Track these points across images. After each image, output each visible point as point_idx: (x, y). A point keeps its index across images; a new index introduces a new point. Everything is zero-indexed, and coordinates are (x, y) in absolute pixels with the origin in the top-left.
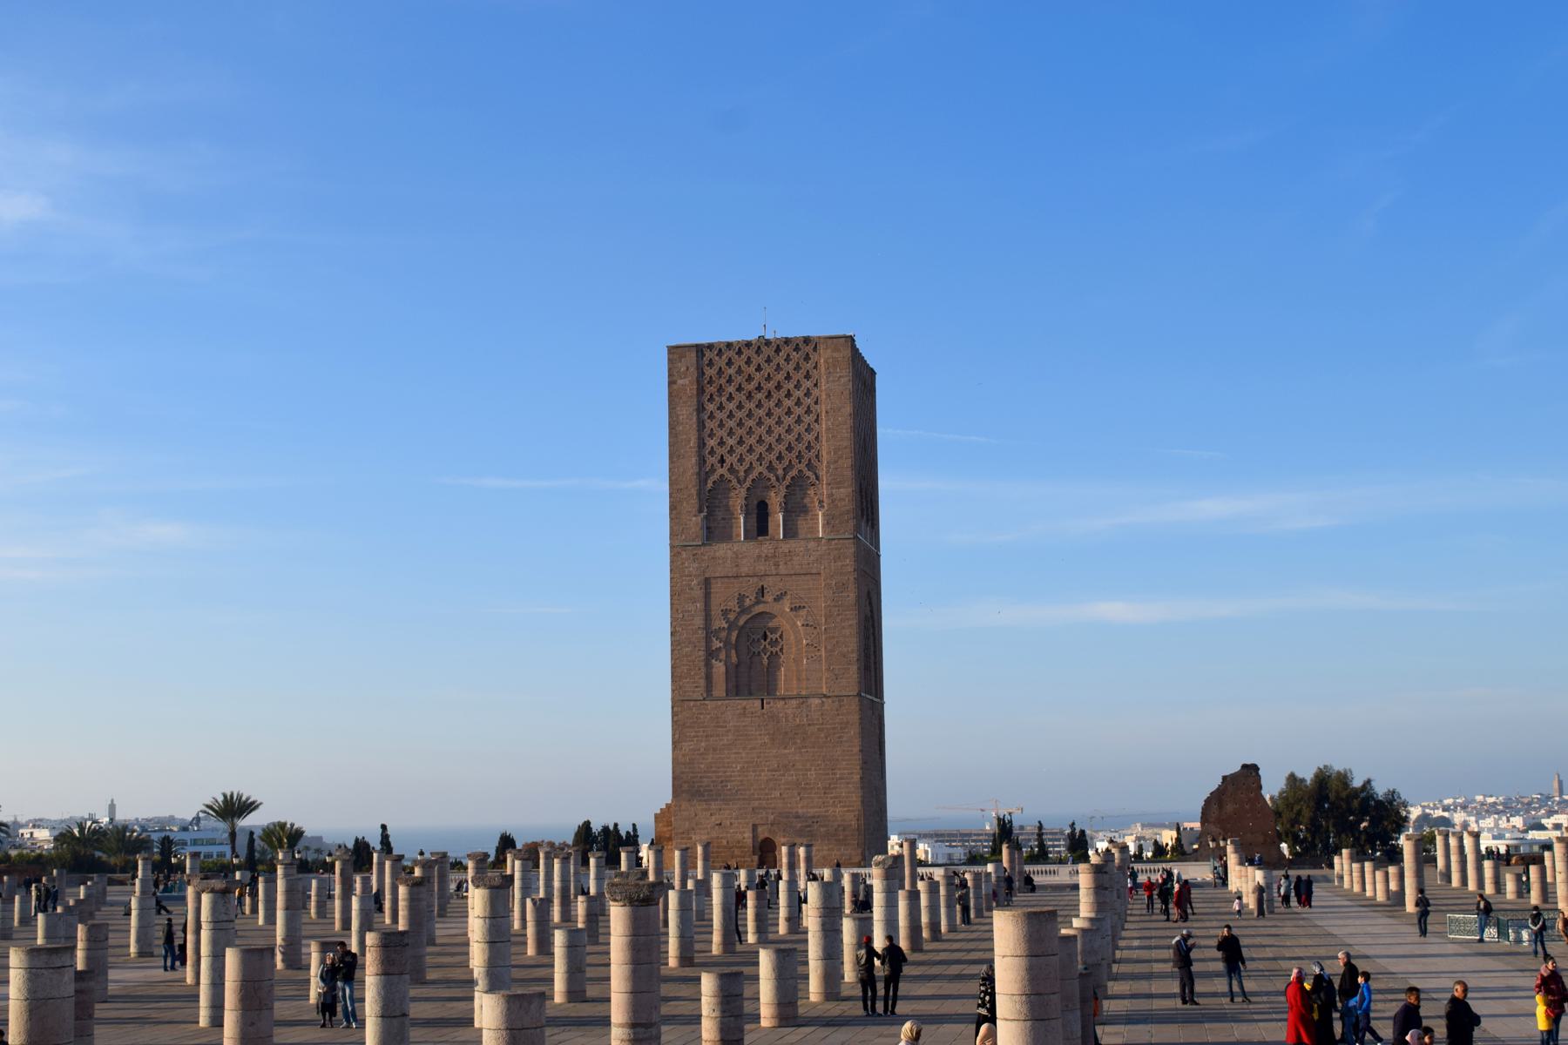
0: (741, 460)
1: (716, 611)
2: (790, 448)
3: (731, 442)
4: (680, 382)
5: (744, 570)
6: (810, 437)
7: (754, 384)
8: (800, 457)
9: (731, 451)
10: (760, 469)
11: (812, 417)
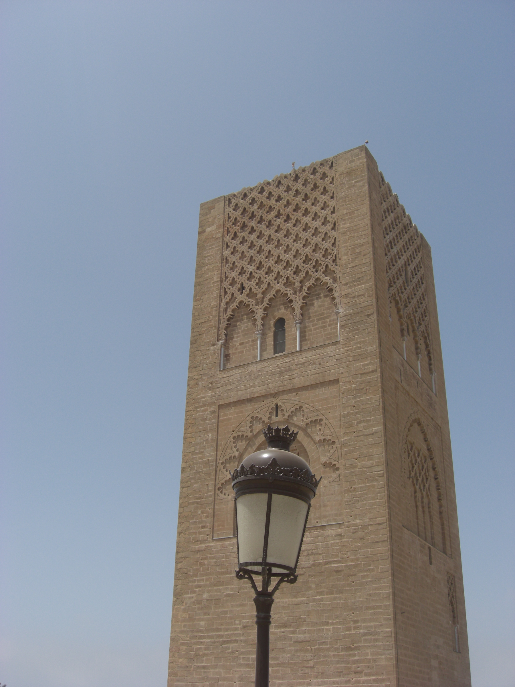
0: (259, 283)
2: (307, 260)
3: (251, 268)
4: (208, 230)
5: (258, 390)
6: (327, 245)
7: (274, 213)
10: (277, 287)
11: (329, 227)
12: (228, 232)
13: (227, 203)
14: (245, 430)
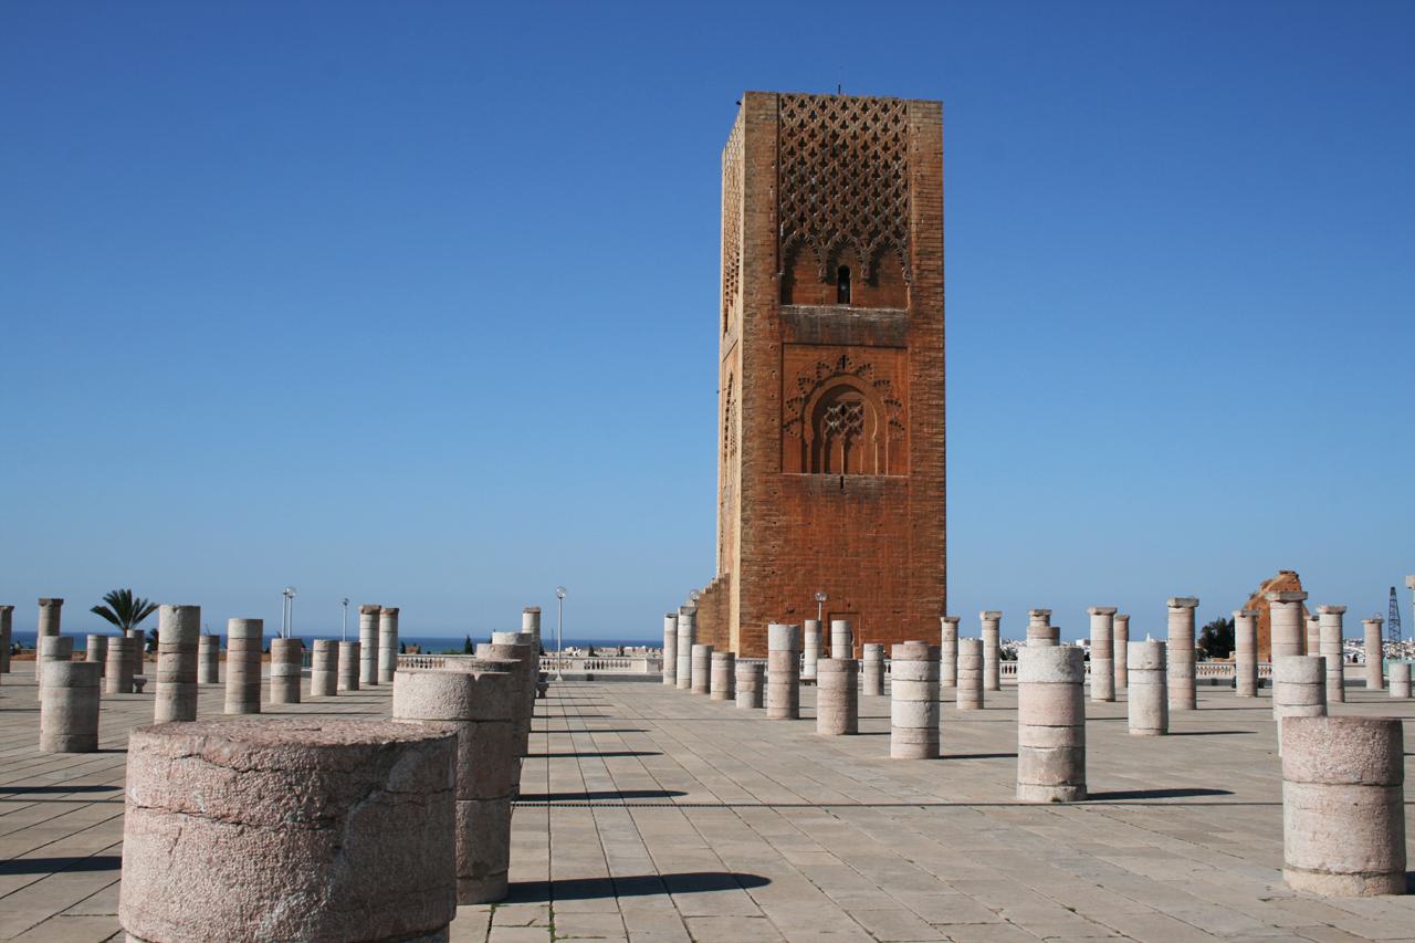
0: (823, 220)
1: (790, 378)
8: (886, 222)
9: (813, 210)
12: (784, 144)
13: (781, 103)
14: (811, 373)
